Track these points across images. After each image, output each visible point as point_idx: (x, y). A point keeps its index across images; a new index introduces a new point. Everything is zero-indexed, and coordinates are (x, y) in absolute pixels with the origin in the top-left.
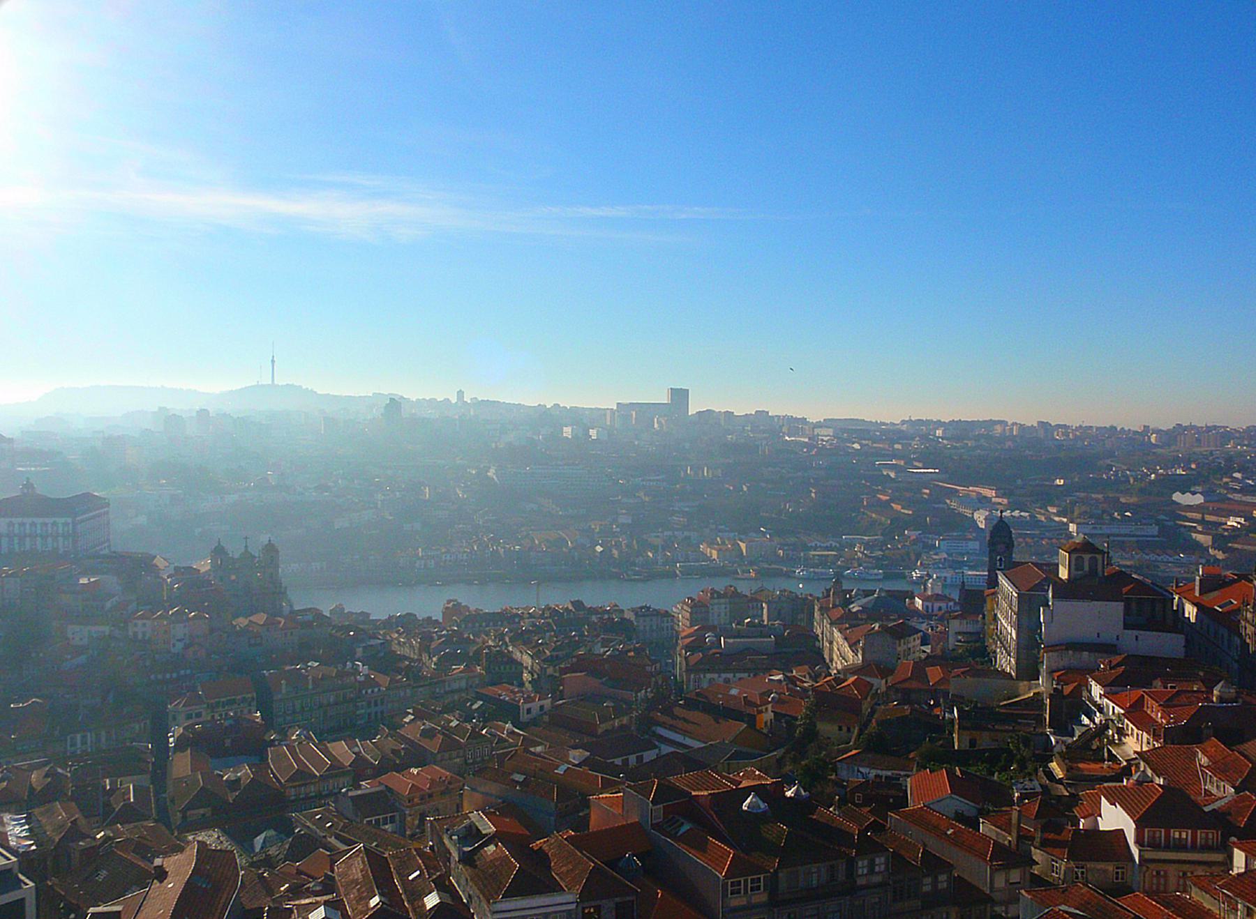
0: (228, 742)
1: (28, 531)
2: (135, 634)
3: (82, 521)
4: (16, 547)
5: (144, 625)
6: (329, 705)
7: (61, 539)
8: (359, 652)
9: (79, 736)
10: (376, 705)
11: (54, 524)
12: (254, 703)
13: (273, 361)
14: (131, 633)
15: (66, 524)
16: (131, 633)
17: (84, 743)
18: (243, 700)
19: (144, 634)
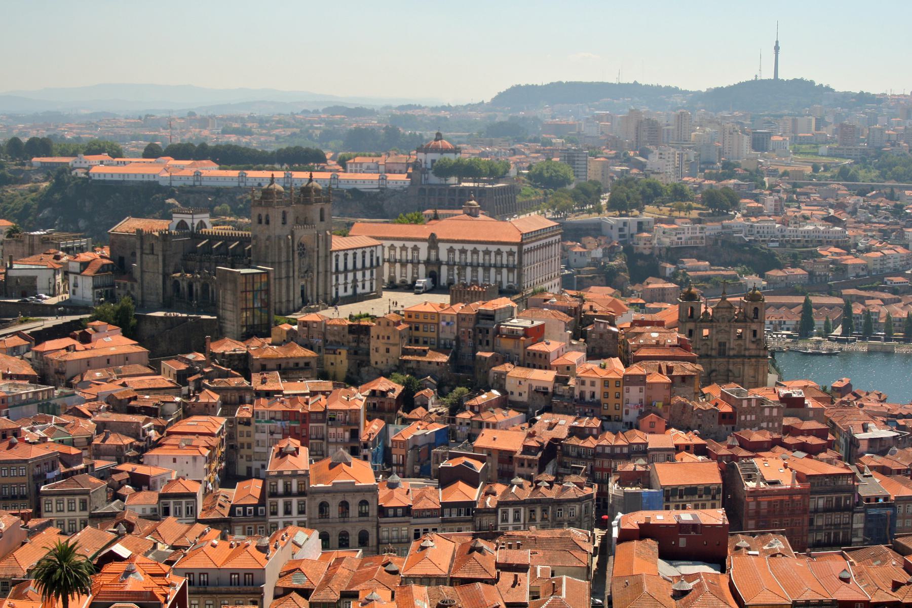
0: (682, 542)
1: (469, 260)
2: (582, 394)
3: (530, 250)
4: (456, 277)
5: (593, 384)
6: (816, 511)
7: (505, 271)
9: (511, 511)
11: (499, 252)
12: (720, 497)
13: (777, 48)
14: (577, 393)
15: (510, 253)
16: (577, 393)
17: (516, 519)
18: (707, 490)
19: (593, 395)
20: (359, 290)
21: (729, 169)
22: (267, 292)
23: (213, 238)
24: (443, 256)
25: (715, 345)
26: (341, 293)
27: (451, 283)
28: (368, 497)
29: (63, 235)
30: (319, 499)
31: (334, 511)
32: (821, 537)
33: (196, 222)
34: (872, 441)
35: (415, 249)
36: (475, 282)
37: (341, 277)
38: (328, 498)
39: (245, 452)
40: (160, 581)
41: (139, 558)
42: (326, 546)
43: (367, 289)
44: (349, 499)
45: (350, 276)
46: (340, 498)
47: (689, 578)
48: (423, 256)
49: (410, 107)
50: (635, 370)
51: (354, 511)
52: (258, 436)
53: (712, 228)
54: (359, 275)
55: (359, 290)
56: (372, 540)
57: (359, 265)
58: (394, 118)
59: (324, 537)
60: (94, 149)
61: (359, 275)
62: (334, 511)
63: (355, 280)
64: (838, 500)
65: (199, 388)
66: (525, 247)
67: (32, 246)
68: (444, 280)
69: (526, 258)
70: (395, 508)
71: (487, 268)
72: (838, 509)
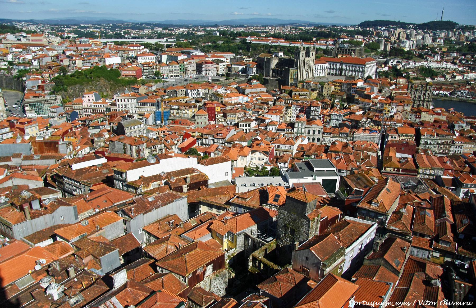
8: (456, 128)
10: (459, 148)
12: (414, 138)
20: (321, 75)
21: (425, 47)
22: (297, 74)
23: (285, 59)
24: (344, 67)
25: (417, 96)
26: (316, 76)
27: (345, 75)
28: (320, 129)
29: (245, 57)
30: (308, 129)
31: (311, 132)
32: (441, 151)
33: (280, 55)
34: (459, 126)
35: (337, 65)
36: (352, 75)
37: (316, 71)
38: (310, 129)
39: (289, 115)
40: (268, 146)
41: (264, 140)
42: (309, 141)
43: (323, 75)
44: (315, 129)
45: (319, 71)
46: (313, 129)
47: (404, 158)
48: (338, 67)
49: (335, 26)
50: (395, 101)
51: (317, 132)
52: (292, 111)
53: (418, 64)
54: (321, 71)
55: (321, 75)
56: (321, 141)
57: (321, 68)
58: (331, 29)
59: (309, 139)
60: (252, 35)
61: (321, 71)
62: (311, 132)
63: (320, 72)
64: (447, 142)
65: (279, 98)
66: (366, 66)
67: (237, 60)
68: (343, 74)
69: (366, 69)
70: (327, 133)
71: (355, 72)
72: (447, 144)
